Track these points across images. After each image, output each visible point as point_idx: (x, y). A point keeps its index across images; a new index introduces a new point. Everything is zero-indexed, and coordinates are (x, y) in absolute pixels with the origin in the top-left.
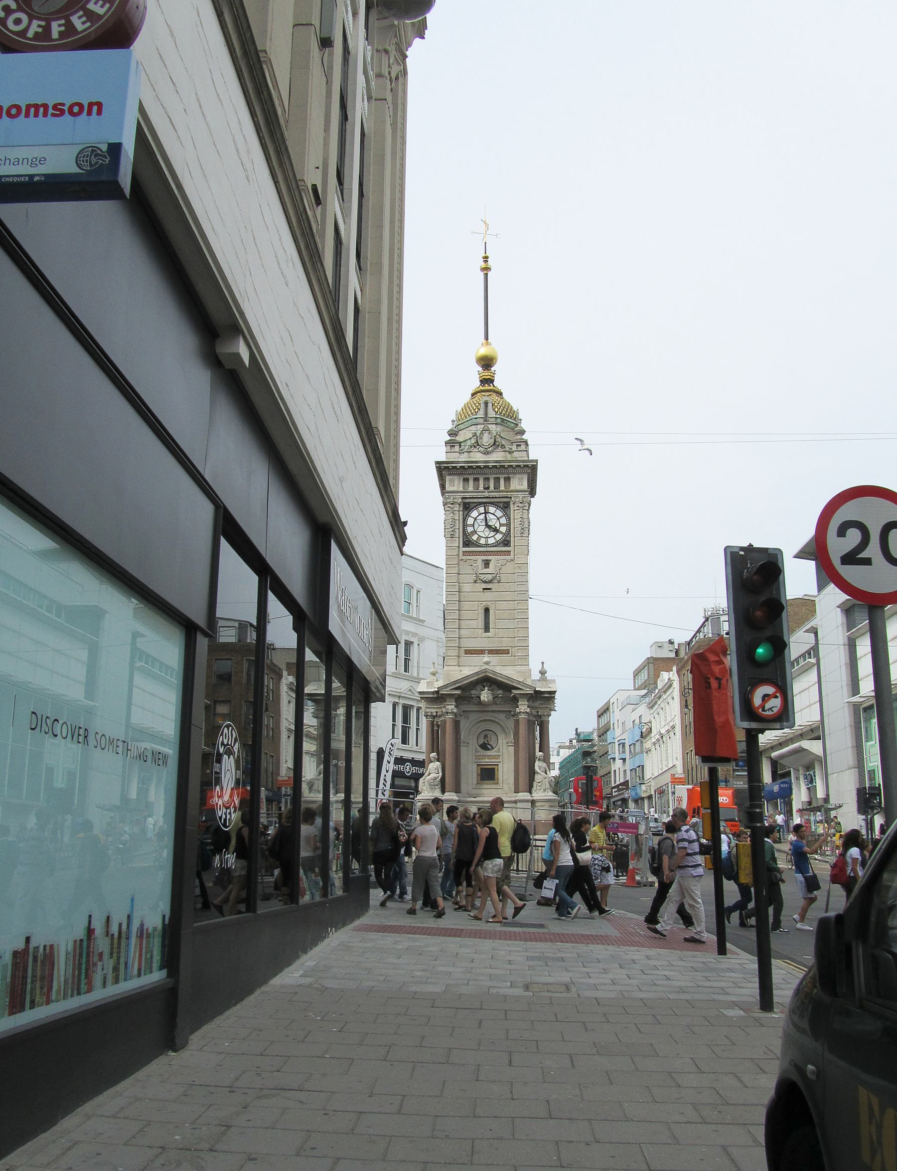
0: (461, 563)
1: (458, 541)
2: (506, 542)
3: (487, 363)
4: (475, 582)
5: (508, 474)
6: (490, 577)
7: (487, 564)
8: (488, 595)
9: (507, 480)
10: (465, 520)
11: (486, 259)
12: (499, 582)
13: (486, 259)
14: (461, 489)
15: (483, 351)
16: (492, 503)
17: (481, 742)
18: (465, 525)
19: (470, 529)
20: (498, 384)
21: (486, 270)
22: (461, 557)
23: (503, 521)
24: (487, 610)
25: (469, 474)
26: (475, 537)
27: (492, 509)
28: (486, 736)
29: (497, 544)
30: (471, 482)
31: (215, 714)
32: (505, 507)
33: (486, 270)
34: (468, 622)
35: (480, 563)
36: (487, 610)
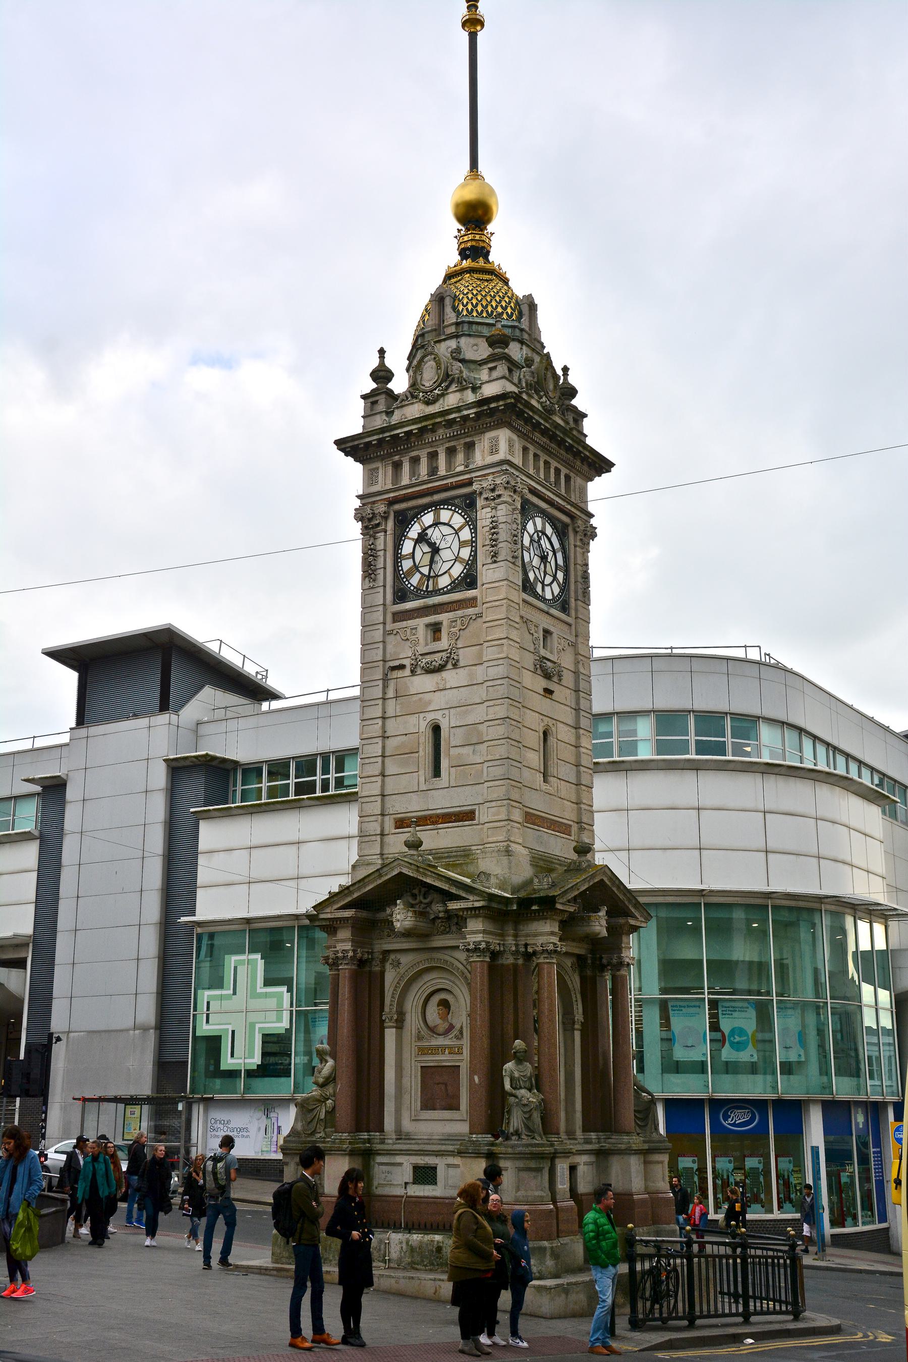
0: (390, 639)
1: (384, 594)
2: (469, 580)
3: (474, 216)
7: (436, 629)
10: (398, 546)
12: (455, 666)
15: (470, 194)
16: (445, 502)
18: (398, 558)
19: (407, 565)
20: (500, 255)
22: (389, 627)
23: (466, 534)
26: (415, 580)
27: (445, 515)
29: (455, 586)
30: (406, 467)
31: (141, 1105)
32: (468, 505)
35: (422, 633)
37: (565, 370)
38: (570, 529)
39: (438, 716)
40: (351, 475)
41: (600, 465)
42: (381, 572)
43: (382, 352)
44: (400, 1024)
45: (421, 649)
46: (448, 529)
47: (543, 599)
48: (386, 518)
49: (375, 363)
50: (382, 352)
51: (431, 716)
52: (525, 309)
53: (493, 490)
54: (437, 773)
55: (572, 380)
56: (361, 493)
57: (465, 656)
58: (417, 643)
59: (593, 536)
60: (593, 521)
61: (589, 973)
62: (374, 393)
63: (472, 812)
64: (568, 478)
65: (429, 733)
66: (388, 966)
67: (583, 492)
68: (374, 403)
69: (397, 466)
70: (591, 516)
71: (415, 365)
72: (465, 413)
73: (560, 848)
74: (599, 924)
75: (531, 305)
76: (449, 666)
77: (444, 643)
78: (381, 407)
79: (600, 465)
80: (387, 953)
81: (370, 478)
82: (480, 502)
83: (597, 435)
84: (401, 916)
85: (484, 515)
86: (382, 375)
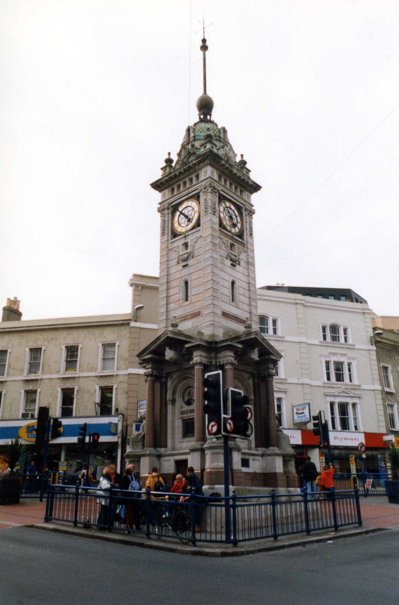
3: (205, 106)
4: (178, 263)
5: (196, 171)
6: (186, 255)
8: (186, 271)
9: (197, 177)
11: (204, 41)
12: (193, 257)
13: (204, 41)
14: (170, 196)
17: (186, 399)
21: (204, 48)
22: (170, 248)
24: (186, 283)
25: (174, 184)
28: (189, 393)
29: (193, 228)
33: (204, 48)
34: (174, 297)
36: (186, 283)
37: (242, 156)
38: (243, 209)
39: (187, 277)
40: (157, 196)
41: (256, 188)
42: (167, 229)
43: (169, 154)
44: (173, 401)
45: (181, 253)
46: (191, 208)
47: (230, 232)
48: (170, 209)
49: (167, 157)
50: (169, 154)
51: (184, 278)
52: (222, 131)
53: (205, 189)
54: (187, 300)
55: (245, 158)
56: (160, 201)
57: (196, 253)
58: (179, 252)
59: (254, 213)
60: (253, 208)
61: (256, 380)
62: (166, 167)
63: (200, 312)
64: (241, 192)
65: (183, 285)
66: (169, 379)
67: (249, 197)
68: (165, 170)
69: (173, 190)
70: (252, 206)
71: (179, 155)
72: (194, 162)
73: (241, 329)
74: (255, 356)
75: (224, 130)
76: (191, 257)
77: (189, 250)
78: (168, 170)
79: (256, 188)
80: (169, 373)
81: (164, 196)
82: (201, 194)
83: (254, 177)
84: (169, 354)
85: (202, 199)
86: (169, 161)
